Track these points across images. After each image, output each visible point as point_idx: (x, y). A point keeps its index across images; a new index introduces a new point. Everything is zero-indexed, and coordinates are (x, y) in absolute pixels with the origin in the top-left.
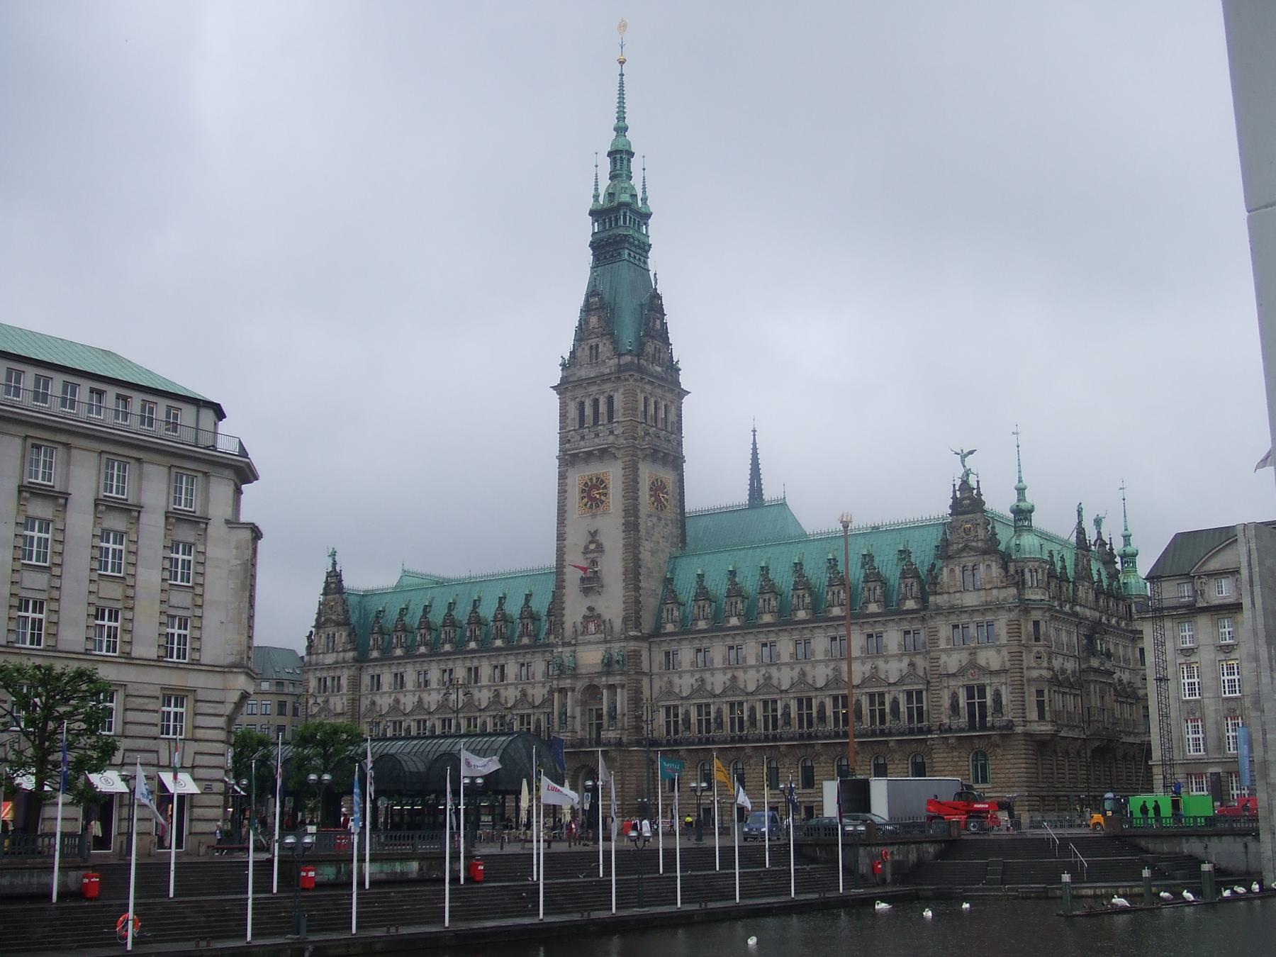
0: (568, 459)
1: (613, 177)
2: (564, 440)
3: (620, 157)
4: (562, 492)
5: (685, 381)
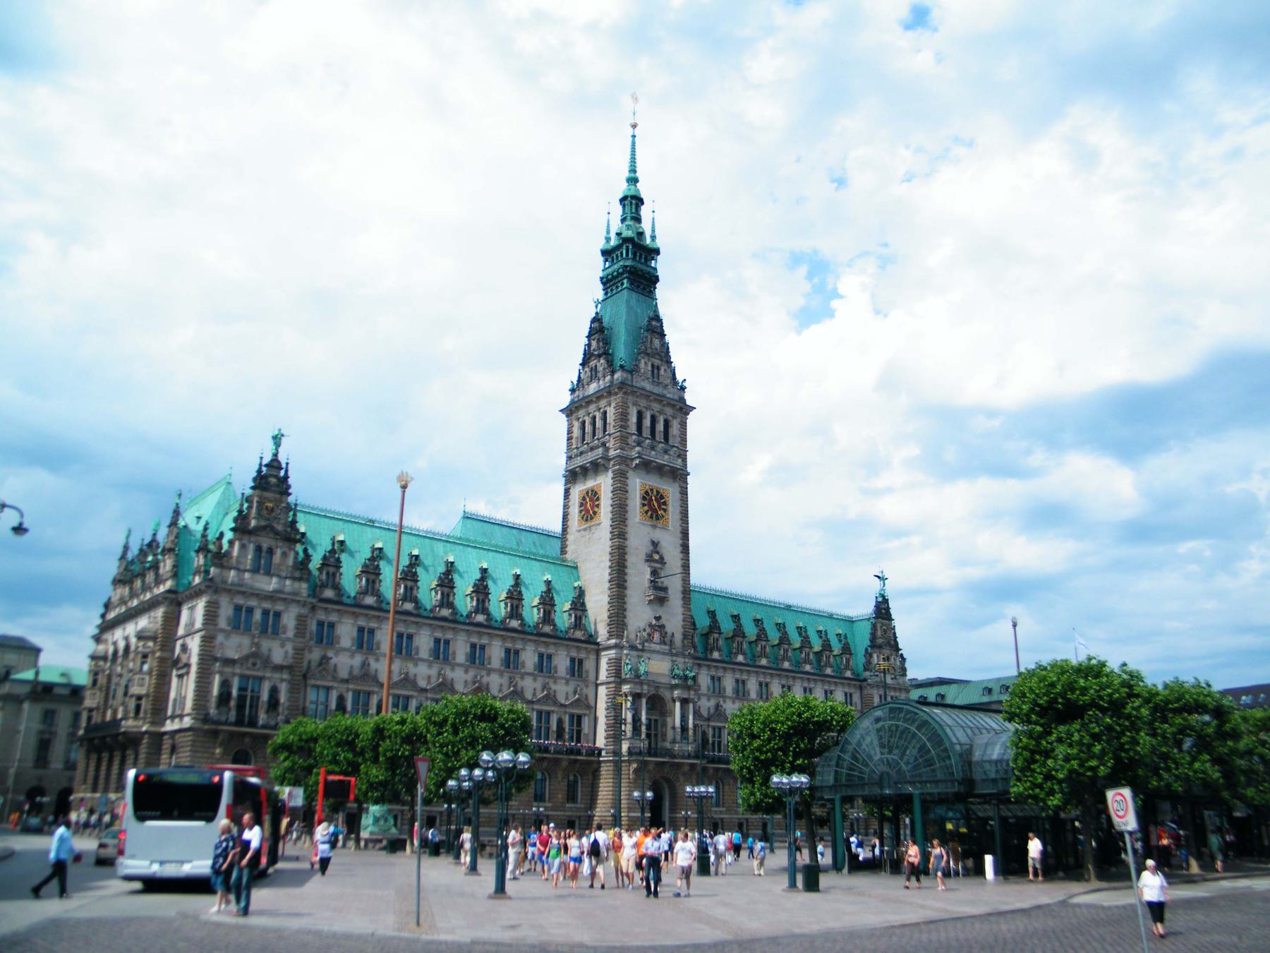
0: (573, 476)
1: (623, 220)
2: (569, 458)
3: (633, 202)
4: (566, 507)
5: (690, 399)
